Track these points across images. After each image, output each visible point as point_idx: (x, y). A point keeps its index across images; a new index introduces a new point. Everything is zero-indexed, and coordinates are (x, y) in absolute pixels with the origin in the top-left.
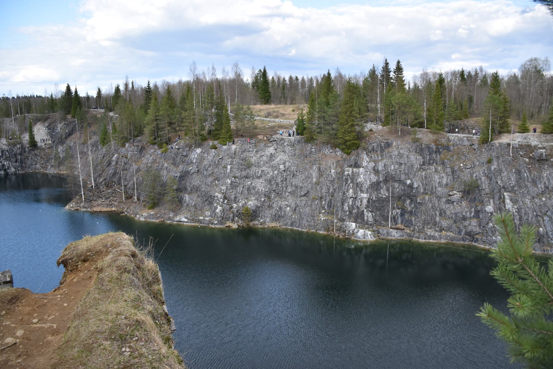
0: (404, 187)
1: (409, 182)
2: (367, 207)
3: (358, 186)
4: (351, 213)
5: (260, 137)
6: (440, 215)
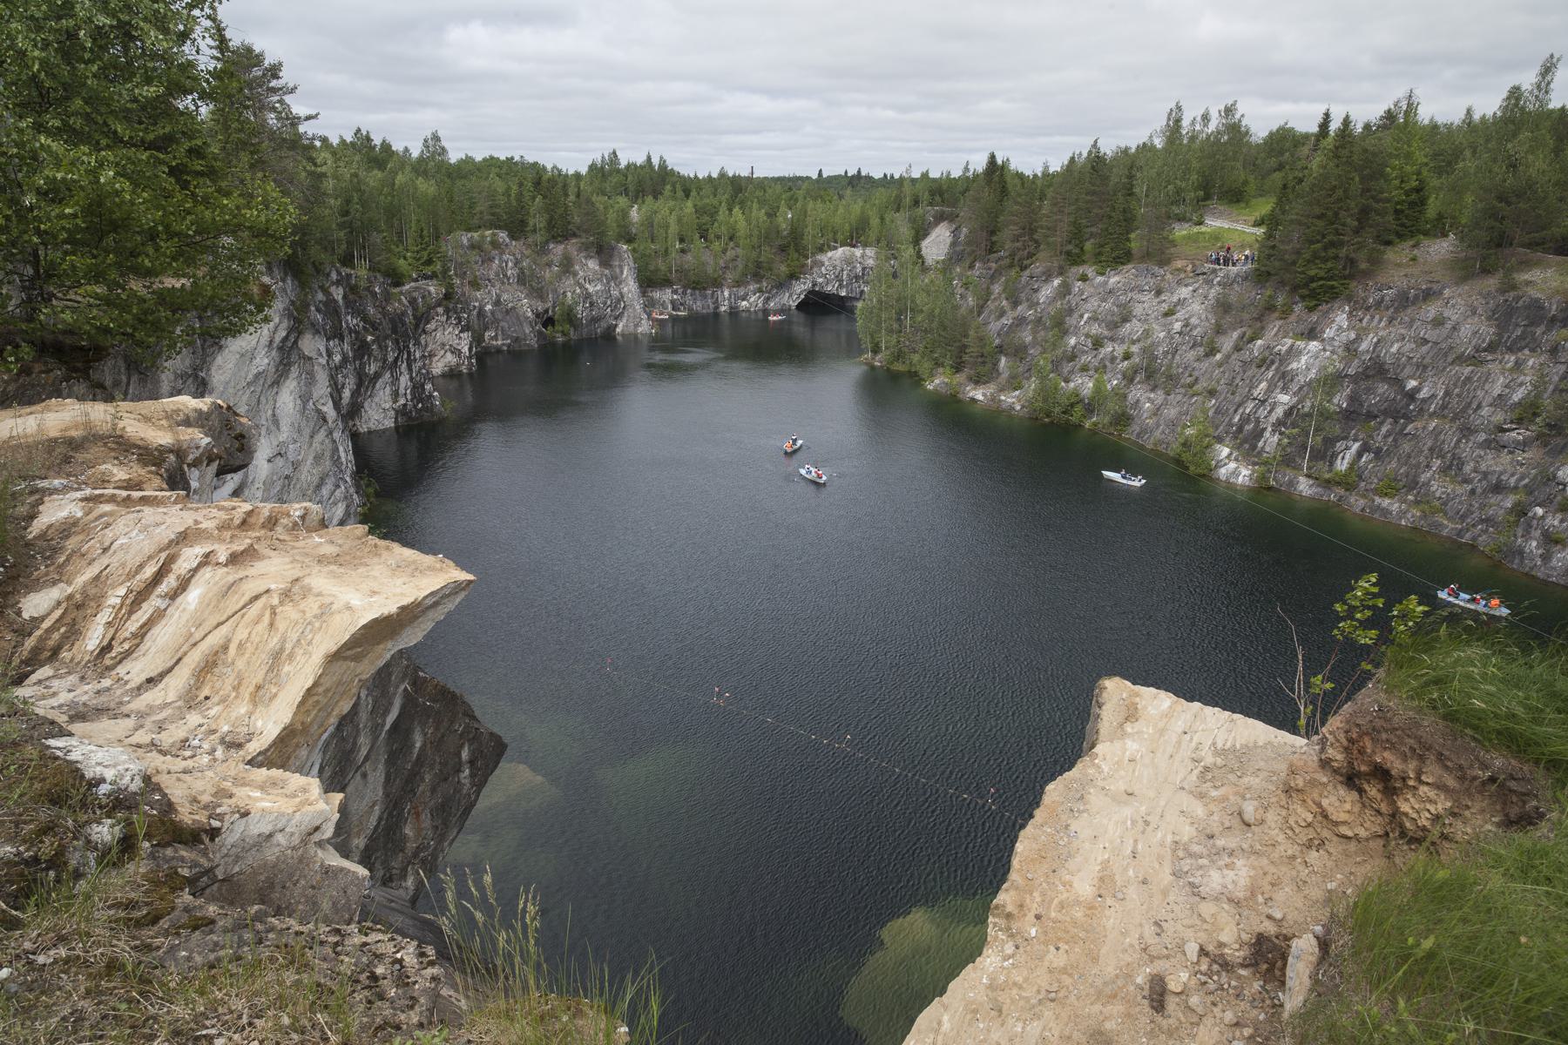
0: (1397, 393)
1: (1412, 383)
2: (1280, 423)
3: (1285, 379)
4: (1240, 429)
5: (1179, 264)
6: (1444, 470)
